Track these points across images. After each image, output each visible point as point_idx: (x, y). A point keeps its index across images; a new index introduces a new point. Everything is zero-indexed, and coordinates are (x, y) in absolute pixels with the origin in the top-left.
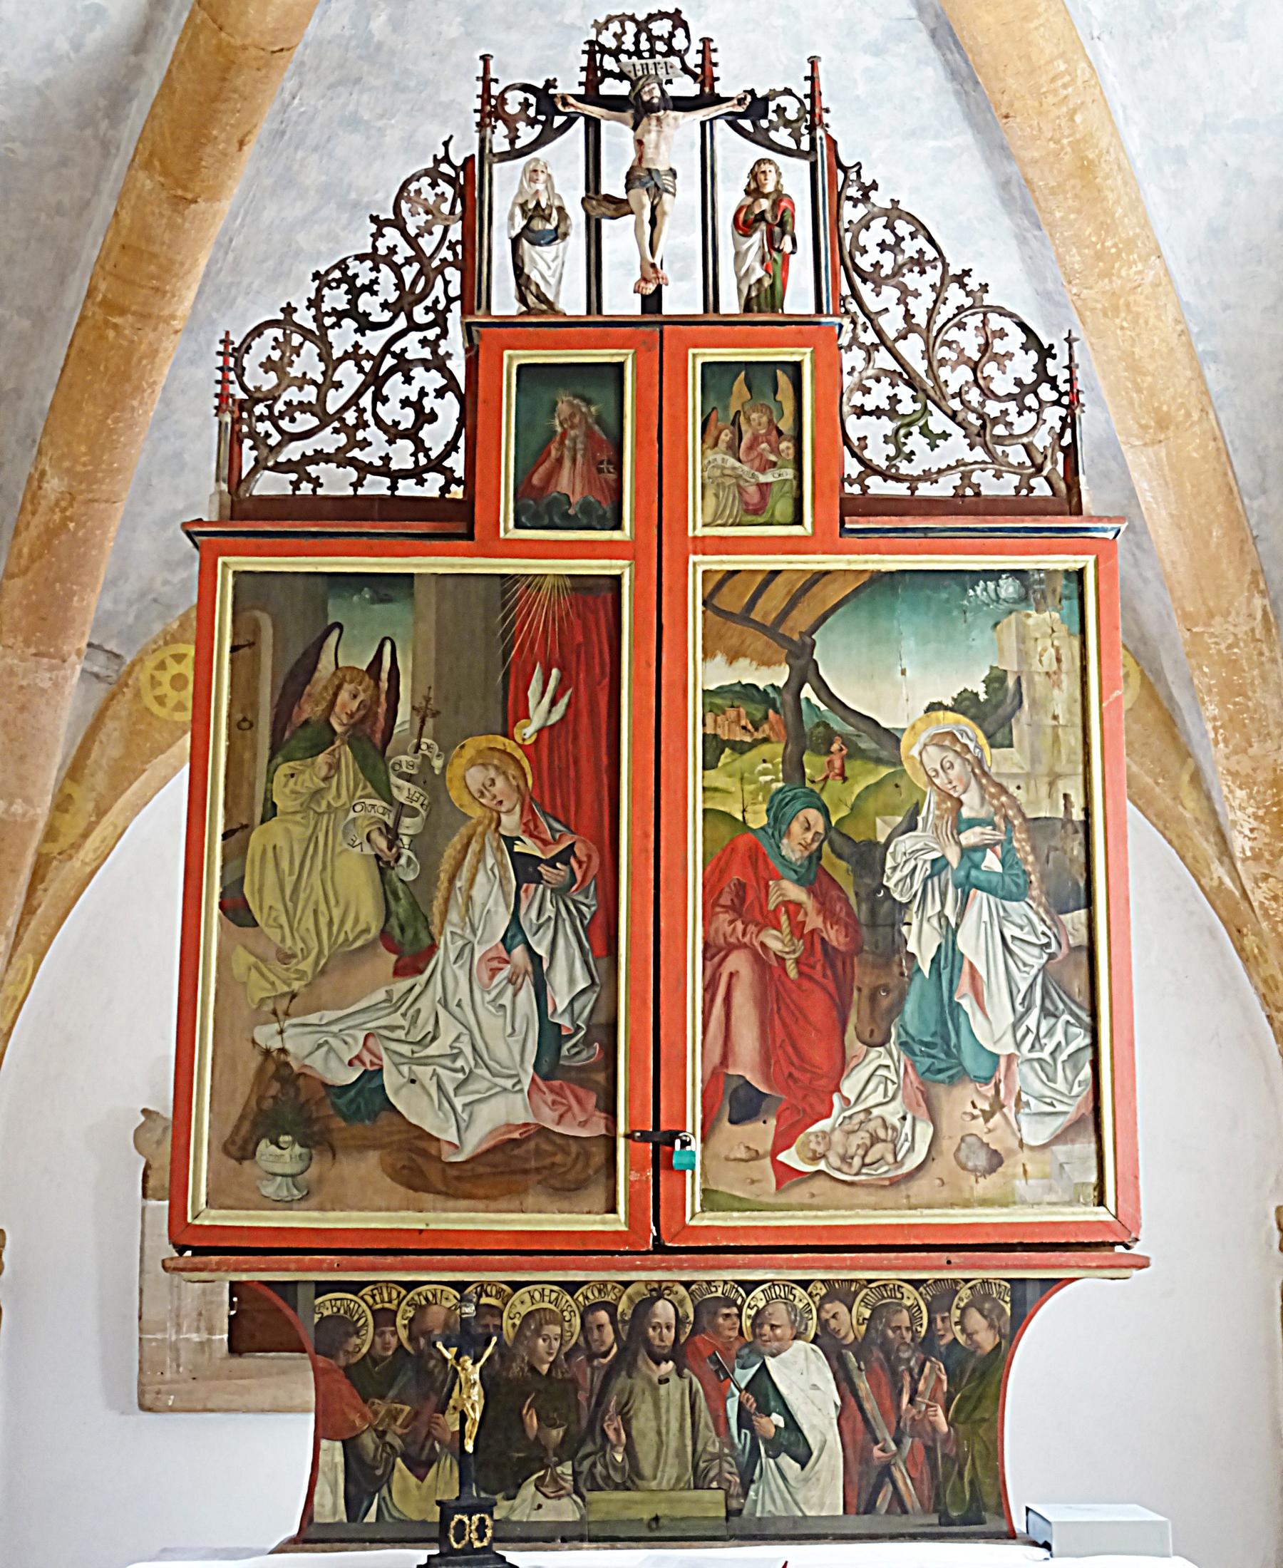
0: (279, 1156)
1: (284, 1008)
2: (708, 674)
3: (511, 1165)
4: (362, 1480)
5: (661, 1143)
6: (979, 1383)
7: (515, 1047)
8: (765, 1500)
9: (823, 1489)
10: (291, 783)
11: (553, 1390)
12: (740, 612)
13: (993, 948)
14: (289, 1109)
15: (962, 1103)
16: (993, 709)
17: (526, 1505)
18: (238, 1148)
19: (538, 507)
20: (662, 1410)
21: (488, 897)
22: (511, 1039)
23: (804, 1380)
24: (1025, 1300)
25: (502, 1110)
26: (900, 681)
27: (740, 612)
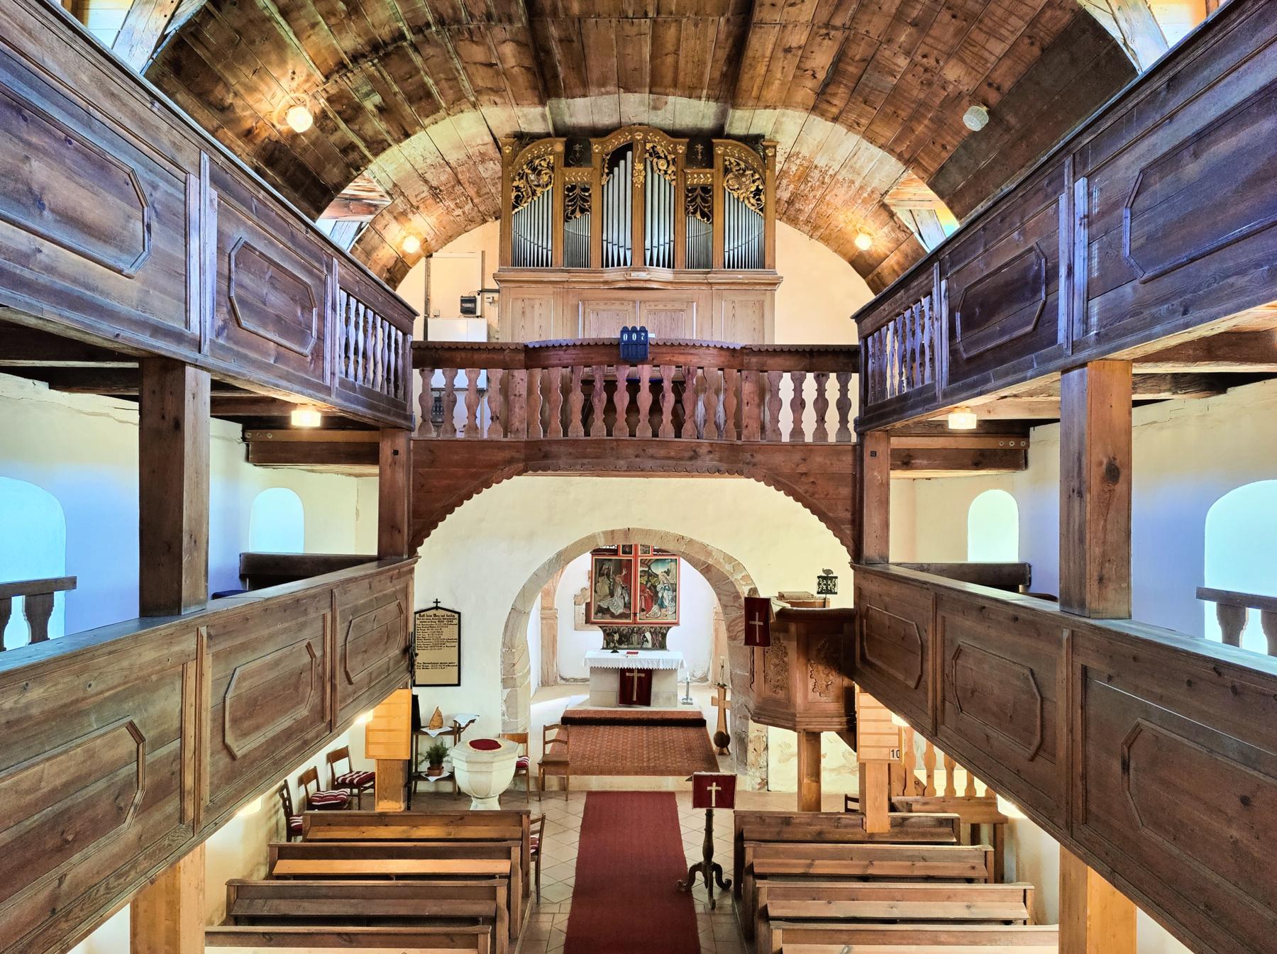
2: (640, 569)
3: (622, 616)
4: (608, 644)
6: (664, 636)
7: (622, 604)
9: (650, 645)
10: (600, 579)
11: (625, 636)
12: (643, 563)
13: (667, 595)
14: (601, 610)
16: (668, 572)
19: (624, 552)
20: (635, 638)
21: (619, 590)
23: (648, 635)
26: (658, 570)
27: (643, 563)
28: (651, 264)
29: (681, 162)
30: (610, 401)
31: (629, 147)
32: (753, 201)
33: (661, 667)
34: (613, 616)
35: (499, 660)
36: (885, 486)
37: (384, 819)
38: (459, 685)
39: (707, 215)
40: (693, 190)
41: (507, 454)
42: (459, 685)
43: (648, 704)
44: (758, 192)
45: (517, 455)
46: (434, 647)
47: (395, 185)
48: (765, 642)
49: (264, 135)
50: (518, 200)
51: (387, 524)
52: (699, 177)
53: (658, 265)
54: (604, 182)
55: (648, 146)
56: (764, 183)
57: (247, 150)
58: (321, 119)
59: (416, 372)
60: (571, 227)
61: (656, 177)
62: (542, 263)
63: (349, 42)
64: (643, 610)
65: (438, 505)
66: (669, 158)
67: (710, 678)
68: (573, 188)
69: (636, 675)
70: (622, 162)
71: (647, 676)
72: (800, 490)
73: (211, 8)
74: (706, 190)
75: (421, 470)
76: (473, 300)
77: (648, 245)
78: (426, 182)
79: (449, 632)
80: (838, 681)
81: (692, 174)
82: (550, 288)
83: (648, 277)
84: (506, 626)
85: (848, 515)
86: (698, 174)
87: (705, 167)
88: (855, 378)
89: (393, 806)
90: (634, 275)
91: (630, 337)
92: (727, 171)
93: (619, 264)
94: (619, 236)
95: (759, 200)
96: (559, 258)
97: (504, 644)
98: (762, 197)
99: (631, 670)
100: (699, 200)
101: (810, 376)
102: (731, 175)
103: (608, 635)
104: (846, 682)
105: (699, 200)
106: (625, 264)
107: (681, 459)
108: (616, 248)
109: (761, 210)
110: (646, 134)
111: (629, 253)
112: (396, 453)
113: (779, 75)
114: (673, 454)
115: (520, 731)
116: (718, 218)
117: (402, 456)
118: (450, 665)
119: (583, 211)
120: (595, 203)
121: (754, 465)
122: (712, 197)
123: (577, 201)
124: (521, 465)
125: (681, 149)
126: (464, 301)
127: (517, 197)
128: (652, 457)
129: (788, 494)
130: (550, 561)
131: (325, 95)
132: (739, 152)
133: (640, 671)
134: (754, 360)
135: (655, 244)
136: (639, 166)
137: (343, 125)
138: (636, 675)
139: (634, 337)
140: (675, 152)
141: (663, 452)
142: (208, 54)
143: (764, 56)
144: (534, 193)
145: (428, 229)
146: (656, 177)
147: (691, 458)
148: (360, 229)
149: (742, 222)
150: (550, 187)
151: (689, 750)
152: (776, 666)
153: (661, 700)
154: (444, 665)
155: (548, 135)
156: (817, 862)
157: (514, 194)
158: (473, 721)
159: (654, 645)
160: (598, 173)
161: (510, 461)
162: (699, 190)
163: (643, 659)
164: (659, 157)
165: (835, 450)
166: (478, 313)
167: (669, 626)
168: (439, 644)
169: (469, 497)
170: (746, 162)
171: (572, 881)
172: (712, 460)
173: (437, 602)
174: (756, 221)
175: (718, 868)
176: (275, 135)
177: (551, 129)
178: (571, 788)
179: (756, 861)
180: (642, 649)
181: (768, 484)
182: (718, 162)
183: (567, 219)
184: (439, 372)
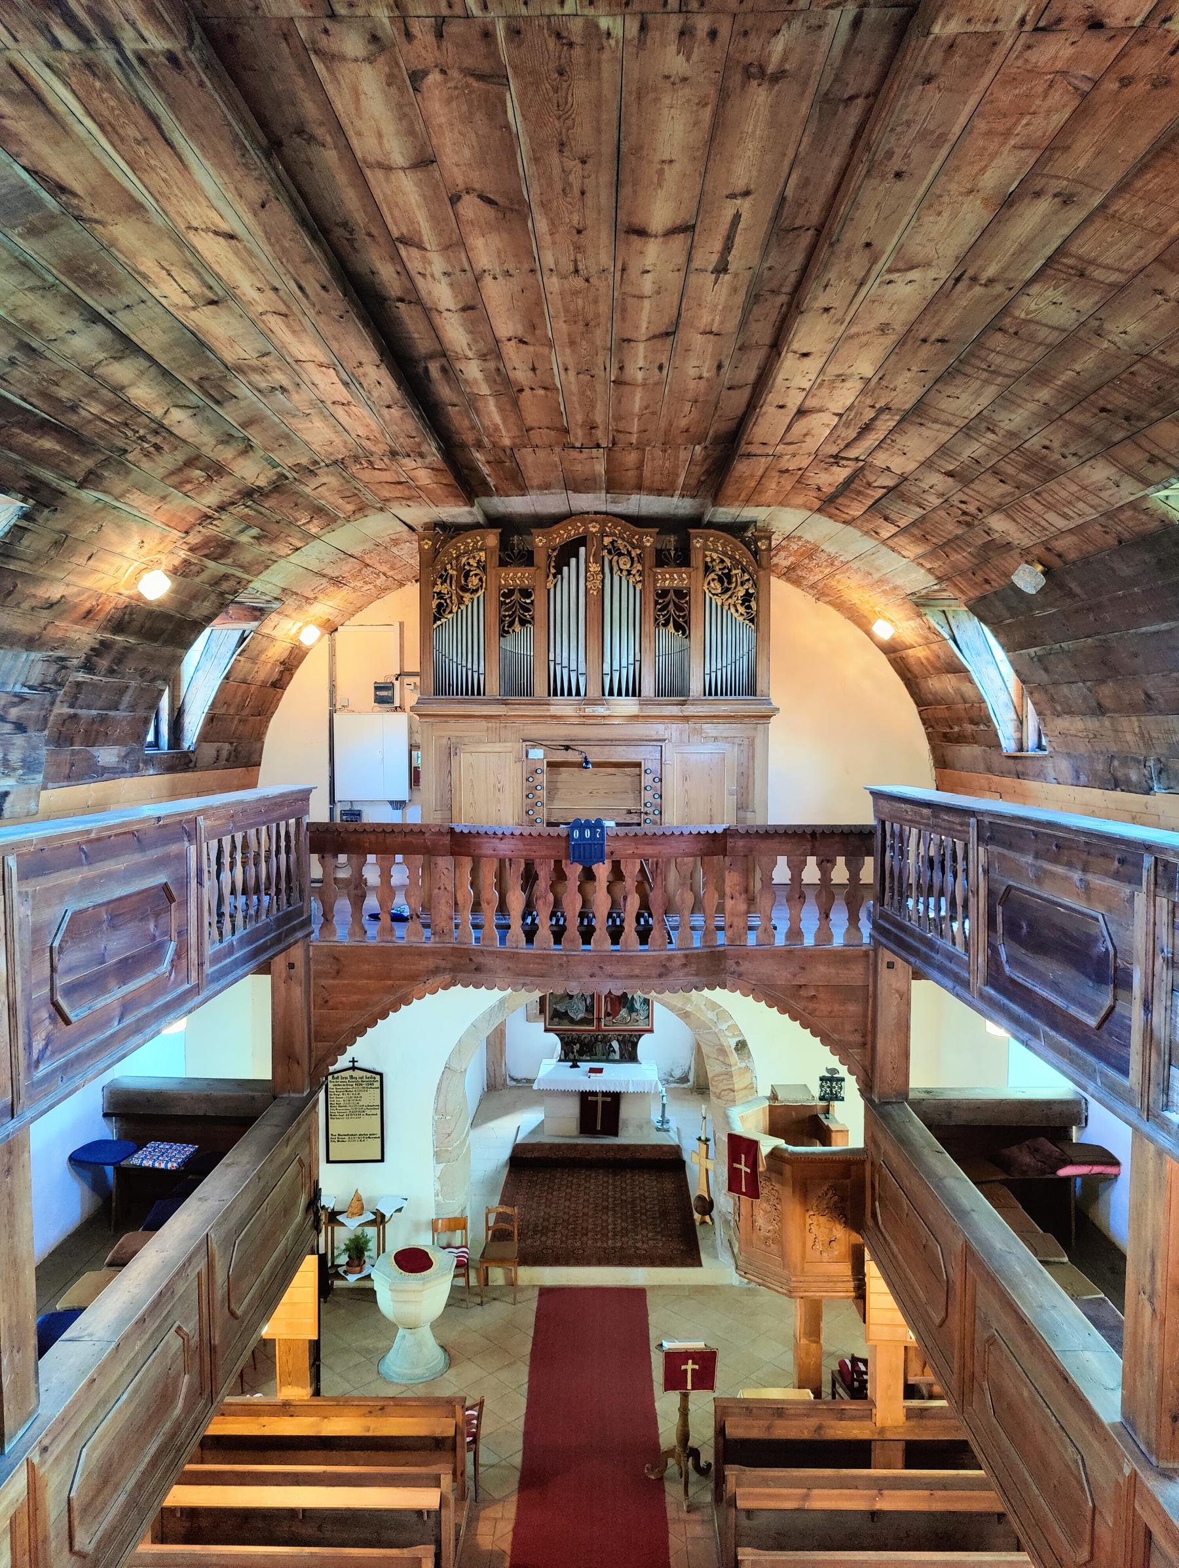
0: (556, 1020)
1: (556, 1003)
3: (583, 1021)
4: (566, 1055)
5: (599, 1019)
6: (635, 1045)
8: (611, 1057)
9: (617, 1057)
11: (587, 1045)
15: (634, 1014)
17: (584, 1058)
18: (551, 1019)
20: (599, 1048)
22: (582, 1007)
23: (615, 1045)
24: (640, 1036)
25: (581, 1015)
28: (611, 693)
29: (650, 560)
30: (557, 903)
31: (582, 541)
32: (741, 609)
33: (631, 1090)
34: (572, 1021)
35: (429, 1130)
36: (905, 998)
37: (286, 1409)
38: (382, 1160)
39: (682, 627)
40: (664, 593)
41: (431, 963)
42: (382, 1160)
43: (616, 1134)
44: (747, 597)
45: (442, 964)
46: (351, 1115)
47: (284, 590)
48: (754, 1193)
49: (109, 607)
50: (441, 610)
51: (283, 1052)
52: (671, 579)
53: (620, 694)
54: (550, 585)
55: (607, 541)
56: (755, 585)
57: (87, 630)
58: (181, 572)
59: (315, 858)
60: (508, 643)
61: (616, 578)
62: (473, 691)
63: (211, 498)
64: (608, 1014)
65: (346, 1026)
66: (633, 554)
67: (691, 1077)
68: (511, 593)
69: (600, 1099)
70: (573, 561)
71: (614, 1100)
72: (798, 1006)
73: (24, 523)
74: (680, 594)
75: (323, 982)
76: (389, 687)
77: (607, 669)
78: (324, 576)
79: (371, 1097)
80: (843, 1236)
81: (663, 574)
82: (484, 724)
83: (607, 713)
84: (439, 1089)
85: (857, 1038)
86: (671, 575)
87: (680, 565)
88: (869, 861)
89: (299, 1393)
90: (589, 710)
91: (582, 834)
92: (708, 569)
93: (570, 694)
94: (570, 656)
95: (748, 607)
96: (493, 687)
97: (436, 1110)
98: (753, 604)
99: (594, 1094)
100: (671, 607)
101: (812, 861)
102: (713, 575)
103: (567, 1044)
104: (857, 1238)
105: (671, 607)
106: (578, 694)
107: (648, 977)
108: (565, 671)
109: (752, 621)
110: (603, 525)
111: (582, 680)
112: (291, 966)
113: (773, 486)
114: (637, 971)
115: (457, 1214)
116: (696, 633)
117: (300, 969)
118: (371, 1136)
119: (523, 623)
120: (539, 612)
121: (740, 975)
122: (688, 603)
123: (516, 611)
124: (448, 977)
125: (648, 542)
126: (377, 688)
127: (439, 606)
128: (611, 976)
129: (782, 1011)
130: (492, 1009)
131: (186, 547)
132: (724, 546)
133: (605, 1094)
134: (741, 843)
135: (616, 666)
136: (595, 568)
137: (211, 564)
138: (600, 1099)
139: (588, 834)
140: (640, 546)
141: (624, 970)
142: (26, 564)
143: (752, 476)
144: (461, 601)
145: (331, 610)
146: (616, 578)
147: (660, 976)
148: (242, 639)
149: (728, 637)
150: (481, 593)
151: (664, 1214)
152: (766, 1212)
153: (631, 1129)
154: (363, 1137)
155: (477, 526)
156: (815, 1492)
157: (435, 603)
158: (400, 1210)
159: (622, 1056)
160: (543, 573)
161: (435, 971)
162: (672, 592)
163: (614, 1076)
164: (620, 554)
165: (841, 958)
166: (397, 703)
167: (640, 1033)
168: (358, 1112)
169: (384, 1016)
170: (732, 558)
171: (518, 1460)
172: (687, 975)
173: (353, 1061)
174: (746, 632)
175: (695, 1453)
176: (122, 601)
177: (481, 519)
178: (520, 1283)
179: (739, 1491)
180: (608, 1061)
181: (758, 999)
182: (697, 560)
183: (503, 633)
184: (342, 858)
